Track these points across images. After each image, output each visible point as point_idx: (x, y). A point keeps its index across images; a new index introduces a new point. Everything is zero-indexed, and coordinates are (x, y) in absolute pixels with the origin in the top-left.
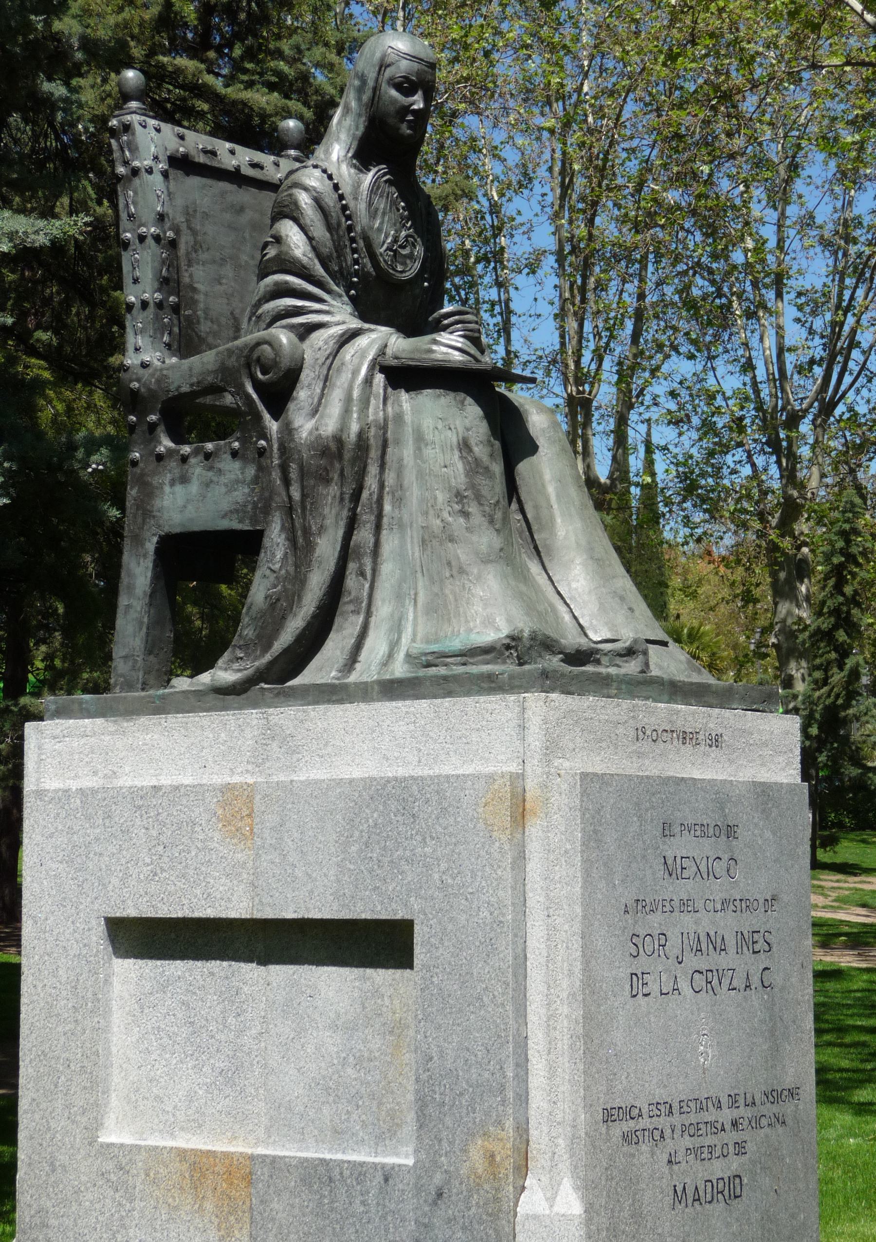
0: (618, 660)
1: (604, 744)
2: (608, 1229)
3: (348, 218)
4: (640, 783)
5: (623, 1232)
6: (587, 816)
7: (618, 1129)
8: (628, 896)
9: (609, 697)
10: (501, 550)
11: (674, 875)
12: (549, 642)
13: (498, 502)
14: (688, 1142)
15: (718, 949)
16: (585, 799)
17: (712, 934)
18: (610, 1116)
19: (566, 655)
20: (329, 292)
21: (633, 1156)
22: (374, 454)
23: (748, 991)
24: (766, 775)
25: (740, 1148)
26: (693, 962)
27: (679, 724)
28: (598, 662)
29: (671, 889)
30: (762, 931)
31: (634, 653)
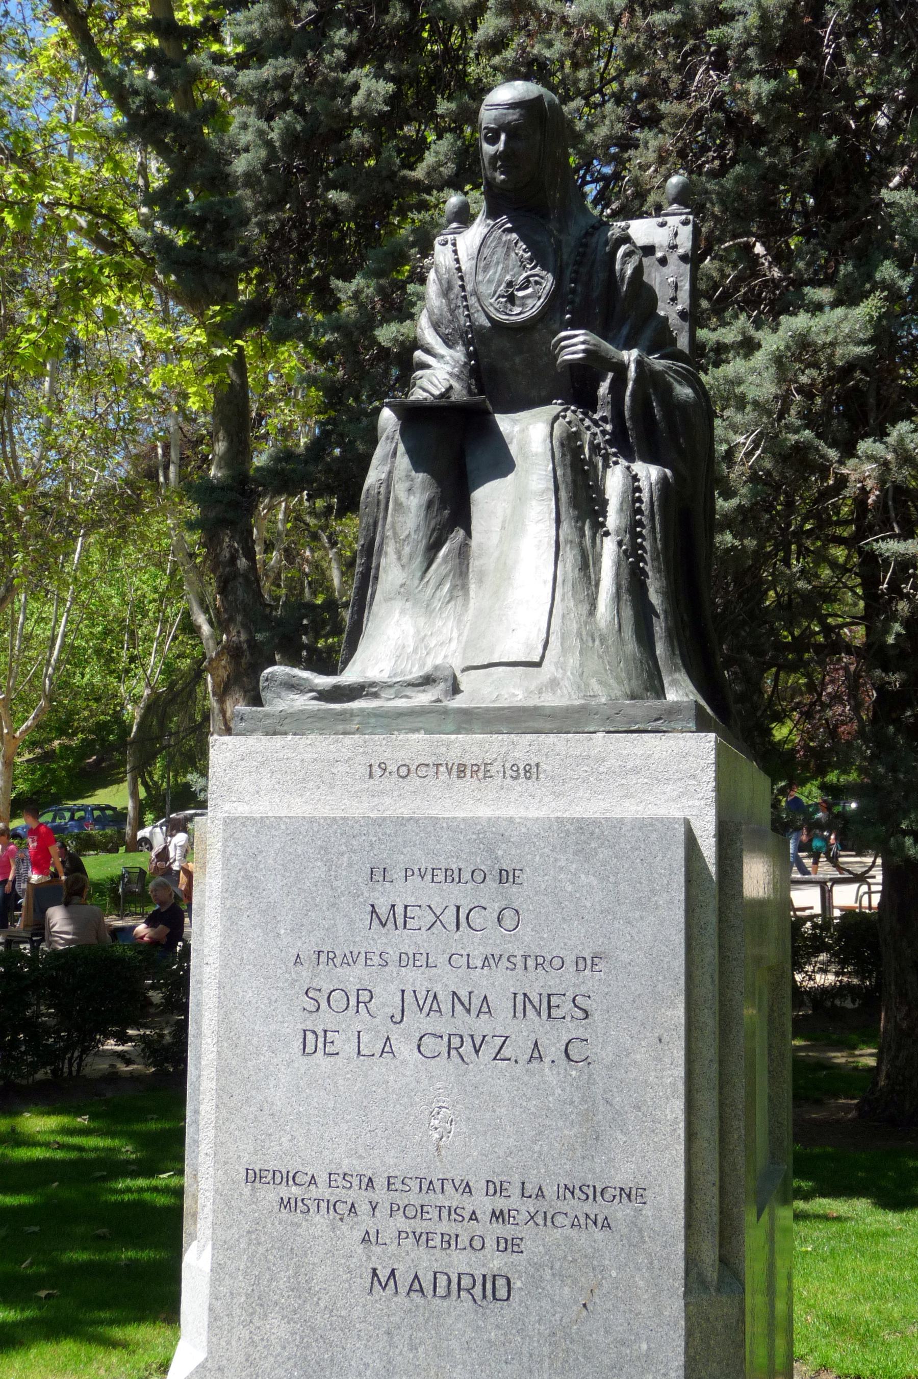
0: (409, 691)
1: (311, 785)
2: (248, 1296)
3: (462, 278)
4: (330, 826)
5: (276, 1303)
6: (234, 861)
7: (270, 1195)
8: (306, 946)
9: (345, 733)
10: (402, 585)
11: (390, 925)
12: (294, 681)
13: (408, 536)
14: (400, 1222)
15: (474, 1012)
16: (231, 844)
17: (463, 994)
18: (255, 1177)
19: (319, 692)
20: (434, 355)
21: (299, 1225)
22: (382, 506)
23: (535, 1064)
24: (633, 808)
25: (509, 1245)
26: (416, 1022)
27: (453, 757)
28: (376, 695)
29: (384, 940)
30: (570, 995)
31: (434, 681)
